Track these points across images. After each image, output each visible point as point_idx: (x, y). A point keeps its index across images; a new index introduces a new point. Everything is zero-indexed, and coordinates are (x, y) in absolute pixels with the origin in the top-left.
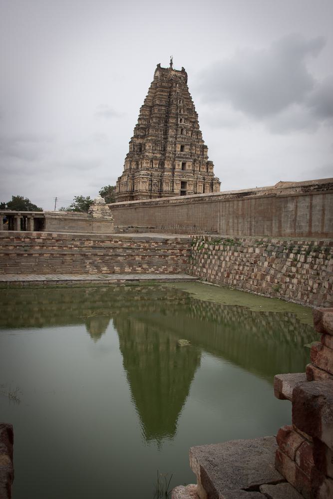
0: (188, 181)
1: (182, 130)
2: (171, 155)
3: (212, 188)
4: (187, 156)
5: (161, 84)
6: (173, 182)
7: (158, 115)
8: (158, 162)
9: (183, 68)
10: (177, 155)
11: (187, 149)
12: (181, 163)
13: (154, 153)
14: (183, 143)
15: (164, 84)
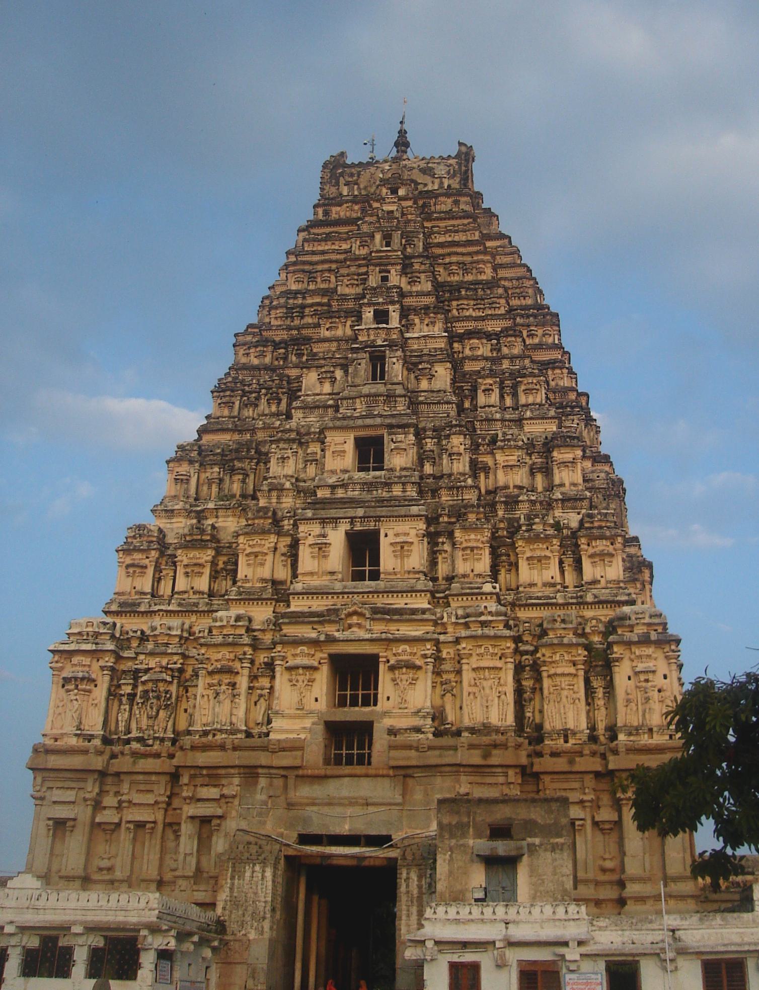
0: (390, 642)
1: (378, 361)
2: (288, 502)
3: (610, 687)
4: (397, 491)
5: (326, 213)
6: (270, 666)
7: (280, 336)
8: (207, 555)
9: (460, 144)
10: (320, 494)
11: (400, 458)
12: (337, 538)
13: (200, 516)
14: (369, 421)
15: (337, 212)
